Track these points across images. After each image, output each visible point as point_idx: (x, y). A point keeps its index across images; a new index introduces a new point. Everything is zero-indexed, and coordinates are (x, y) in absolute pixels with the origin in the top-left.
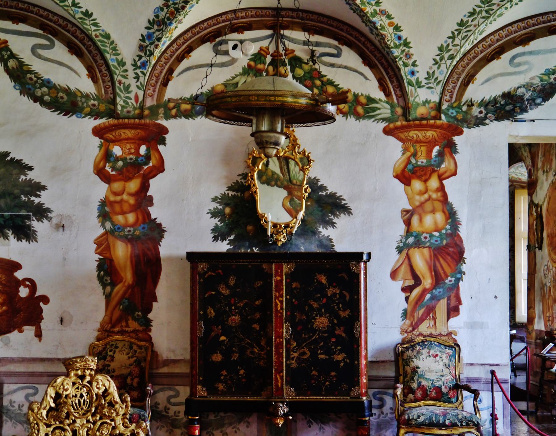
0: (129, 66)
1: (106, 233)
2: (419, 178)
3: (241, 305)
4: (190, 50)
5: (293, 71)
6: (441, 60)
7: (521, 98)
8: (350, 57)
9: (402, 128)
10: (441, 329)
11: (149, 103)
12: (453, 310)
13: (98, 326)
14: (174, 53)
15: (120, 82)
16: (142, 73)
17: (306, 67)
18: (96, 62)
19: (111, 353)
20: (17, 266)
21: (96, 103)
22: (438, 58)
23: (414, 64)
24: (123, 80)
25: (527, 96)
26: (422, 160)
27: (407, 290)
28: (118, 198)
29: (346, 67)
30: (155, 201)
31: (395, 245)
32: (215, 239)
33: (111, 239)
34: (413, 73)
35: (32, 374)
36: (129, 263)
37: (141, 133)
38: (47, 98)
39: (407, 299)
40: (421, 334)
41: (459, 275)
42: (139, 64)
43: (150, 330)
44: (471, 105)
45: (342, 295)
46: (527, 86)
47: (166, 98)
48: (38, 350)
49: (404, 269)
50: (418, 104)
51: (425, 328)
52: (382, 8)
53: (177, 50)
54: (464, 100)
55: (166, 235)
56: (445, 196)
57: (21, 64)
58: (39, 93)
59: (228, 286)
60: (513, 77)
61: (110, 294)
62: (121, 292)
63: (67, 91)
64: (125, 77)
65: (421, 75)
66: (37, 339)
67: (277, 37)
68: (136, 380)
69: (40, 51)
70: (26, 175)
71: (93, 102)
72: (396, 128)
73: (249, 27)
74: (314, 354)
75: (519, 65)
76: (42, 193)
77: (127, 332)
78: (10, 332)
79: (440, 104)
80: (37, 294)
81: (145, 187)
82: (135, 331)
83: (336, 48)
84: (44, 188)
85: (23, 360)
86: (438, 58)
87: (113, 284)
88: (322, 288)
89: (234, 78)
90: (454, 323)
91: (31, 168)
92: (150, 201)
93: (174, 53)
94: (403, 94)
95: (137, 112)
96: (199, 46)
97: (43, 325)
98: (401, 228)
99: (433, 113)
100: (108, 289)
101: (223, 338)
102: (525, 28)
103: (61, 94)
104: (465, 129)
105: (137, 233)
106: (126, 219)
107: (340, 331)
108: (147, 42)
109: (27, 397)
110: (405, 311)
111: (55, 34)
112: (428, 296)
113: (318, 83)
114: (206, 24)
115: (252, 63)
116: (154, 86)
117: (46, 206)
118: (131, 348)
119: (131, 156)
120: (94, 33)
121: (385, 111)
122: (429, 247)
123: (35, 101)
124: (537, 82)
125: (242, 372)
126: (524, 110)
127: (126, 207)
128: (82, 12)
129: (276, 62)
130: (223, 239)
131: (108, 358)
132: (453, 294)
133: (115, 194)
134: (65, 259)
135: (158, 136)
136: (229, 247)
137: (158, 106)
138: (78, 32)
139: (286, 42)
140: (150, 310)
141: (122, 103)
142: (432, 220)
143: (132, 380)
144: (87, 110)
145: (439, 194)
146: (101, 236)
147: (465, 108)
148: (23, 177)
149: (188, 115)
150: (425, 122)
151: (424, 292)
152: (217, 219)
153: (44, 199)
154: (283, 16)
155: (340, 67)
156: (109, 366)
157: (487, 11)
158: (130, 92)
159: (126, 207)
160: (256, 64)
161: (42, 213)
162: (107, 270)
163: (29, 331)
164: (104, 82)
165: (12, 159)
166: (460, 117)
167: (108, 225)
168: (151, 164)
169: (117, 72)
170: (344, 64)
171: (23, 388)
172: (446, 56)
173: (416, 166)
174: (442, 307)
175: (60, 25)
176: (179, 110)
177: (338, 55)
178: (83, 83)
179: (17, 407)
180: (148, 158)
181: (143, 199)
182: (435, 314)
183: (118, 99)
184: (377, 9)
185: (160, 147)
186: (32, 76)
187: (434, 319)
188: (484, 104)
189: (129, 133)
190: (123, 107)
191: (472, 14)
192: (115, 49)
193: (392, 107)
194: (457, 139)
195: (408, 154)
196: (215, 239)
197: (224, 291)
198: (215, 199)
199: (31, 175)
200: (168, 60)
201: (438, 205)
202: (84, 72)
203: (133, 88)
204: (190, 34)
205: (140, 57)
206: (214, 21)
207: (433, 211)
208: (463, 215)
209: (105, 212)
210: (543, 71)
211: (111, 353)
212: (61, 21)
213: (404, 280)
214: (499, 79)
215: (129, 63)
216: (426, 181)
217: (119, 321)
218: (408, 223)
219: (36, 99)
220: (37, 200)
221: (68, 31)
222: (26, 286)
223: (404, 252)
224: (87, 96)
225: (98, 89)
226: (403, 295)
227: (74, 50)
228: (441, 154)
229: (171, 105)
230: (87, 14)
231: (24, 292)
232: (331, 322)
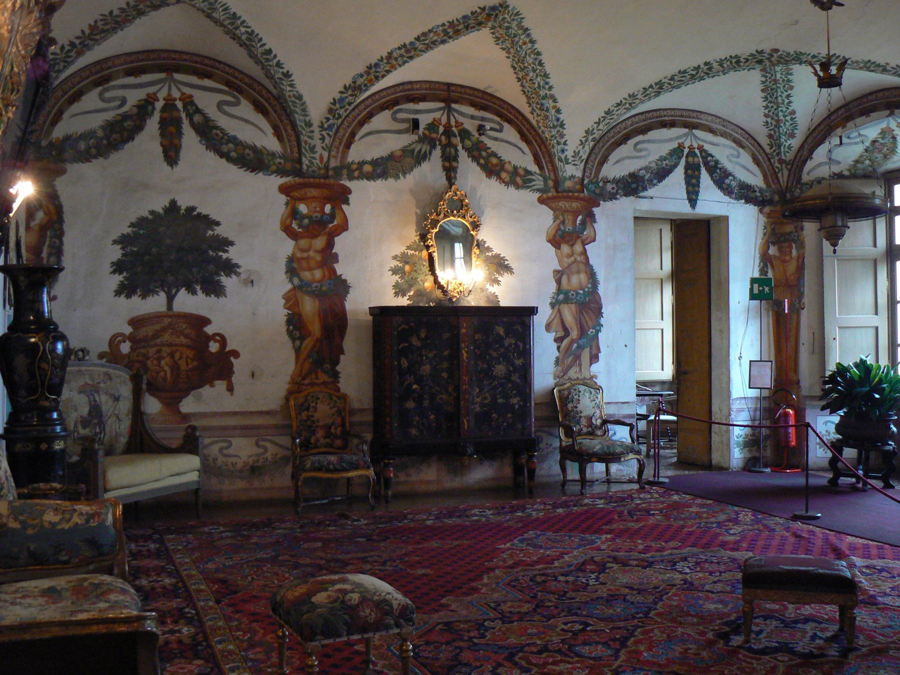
0: (315, 128)
1: (294, 288)
2: (567, 242)
3: (431, 355)
4: (370, 116)
5: (462, 141)
6: (586, 141)
7: (643, 178)
8: (510, 133)
9: (553, 198)
10: (585, 374)
11: (333, 163)
12: (594, 358)
13: (288, 379)
14: (355, 118)
15: (306, 142)
16: (328, 134)
17: (474, 139)
18: (282, 121)
19: (313, 404)
20: (206, 321)
21: (282, 161)
22: (584, 140)
23: (565, 144)
24: (309, 141)
25: (646, 177)
26: (569, 227)
27: (558, 340)
28: (305, 255)
29: (507, 142)
30: (340, 258)
31: (549, 301)
32: (396, 294)
33: (299, 294)
34: (563, 151)
35: (225, 428)
36: (317, 318)
37: (326, 192)
38: (233, 154)
39: (558, 348)
40: (570, 379)
41: (598, 327)
42: (326, 126)
43: (338, 382)
44: (606, 181)
45: (517, 346)
46: (646, 168)
47: (350, 159)
48: (229, 403)
49: (557, 321)
50: (565, 178)
51: (573, 373)
52: (552, 93)
53: (358, 115)
54: (601, 176)
55: (351, 290)
56: (587, 258)
57: (207, 119)
58: (225, 149)
59: (419, 338)
60: (635, 160)
61: (300, 348)
62: (309, 347)
63: (254, 148)
64: (311, 138)
65: (569, 153)
66: (228, 393)
67: (450, 111)
68: (339, 429)
69: (226, 108)
70: (213, 230)
71: (279, 160)
72: (549, 198)
73: (423, 99)
74: (494, 399)
75: (640, 150)
76: (230, 249)
77: (317, 384)
78: (201, 387)
79: (583, 179)
80: (227, 349)
81: (330, 244)
82: (325, 383)
83: (499, 124)
84: (232, 243)
86: (584, 140)
87: (302, 338)
88: (499, 339)
89: (410, 145)
90: (595, 368)
91: (218, 224)
92: (335, 258)
93: (355, 118)
94: (555, 169)
95: (322, 172)
96: (378, 113)
97: (234, 379)
98: (553, 287)
99: (578, 187)
100: (298, 343)
101: (415, 386)
102: (644, 120)
103: (247, 151)
104: (601, 202)
105: (324, 288)
106: (313, 275)
107: (515, 378)
108: (338, 106)
109: (221, 450)
110: (558, 358)
111: (240, 91)
112: (575, 345)
113: (484, 154)
114: (385, 93)
115: (427, 132)
116: (338, 148)
117: (234, 262)
118: (331, 399)
119: (317, 214)
120: (288, 94)
121: (539, 183)
122: (576, 303)
123: (221, 157)
124: (653, 165)
125: (432, 417)
126: (645, 189)
127: (313, 263)
128: (283, 73)
129: (448, 132)
130: (404, 295)
131: (311, 410)
132: (594, 344)
133: (303, 251)
134: (254, 314)
135: (342, 196)
136: (409, 302)
137: (342, 167)
138: (264, 91)
139: (456, 115)
140: (337, 362)
141: (307, 162)
142: (577, 280)
143: (336, 428)
144: (274, 168)
145: (583, 257)
146: (290, 291)
147: (601, 184)
148: (210, 232)
149: (370, 177)
150: (571, 194)
151: (572, 342)
152: (398, 276)
153: (232, 254)
154: (453, 91)
155: (502, 141)
156: (313, 416)
157: (630, 104)
158: (315, 153)
159: (313, 263)
160: (430, 133)
161: (230, 268)
162: (296, 324)
163: (220, 385)
164: (289, 141)
165: (199, 214)
166: (598, 191)
167: (296, 281)
168: (335, 223)
169: (304, 132)
170: (506, 138)
171: (216, 442)
172: (590, 138)
173: (564, 232)
174: (586, 355)
175: (246, 84)
176: (361, 172)
177: (500, 131)
178: (271, 143)
179: (211, 460)
180: (332, 216)
181: (329, 257)
182: (580, 361)
183: (304, 159)
184: (548, 93)
185: (344, 207)
186: (218, 132)
187: (580, 365)
188: (616, 181)
189: (314, 192)
190: (308, 167)
191: (618, 105)
192: (304, 110)
193: (545, 180)
194: (596, 210)
195: (558, 221)
196: (396, 294)
197: (415, 342)
198: (395, 258)
199: (218, 230)
200: (350, 124)
201: (582, 267)
202: (269, 130)
203: (318, 149)
204: (370, 101)
205: (328, 119)
206: (393, 90)
207: (578, 272)
208: (600, 277)
209: (292, 269)
210: (657, 158)
211: (313, 404)
212: (246, 80)
213: (556, 332)
214: (627, 161)
215: (316, 124)
216: (572, 246)
217: (309, 373)
218: (559, 282)
219: (222, 155)
220: (225, 256)
221: (254, 90)
223: (557, 307)
224: (273, 154)
225: (284, 147)
226: (555, 345)
227: (260, 108)
228: (583, 223)
229: (354, 167)
230: (287, 75)
231: (214, 347)
232: (508, 369)
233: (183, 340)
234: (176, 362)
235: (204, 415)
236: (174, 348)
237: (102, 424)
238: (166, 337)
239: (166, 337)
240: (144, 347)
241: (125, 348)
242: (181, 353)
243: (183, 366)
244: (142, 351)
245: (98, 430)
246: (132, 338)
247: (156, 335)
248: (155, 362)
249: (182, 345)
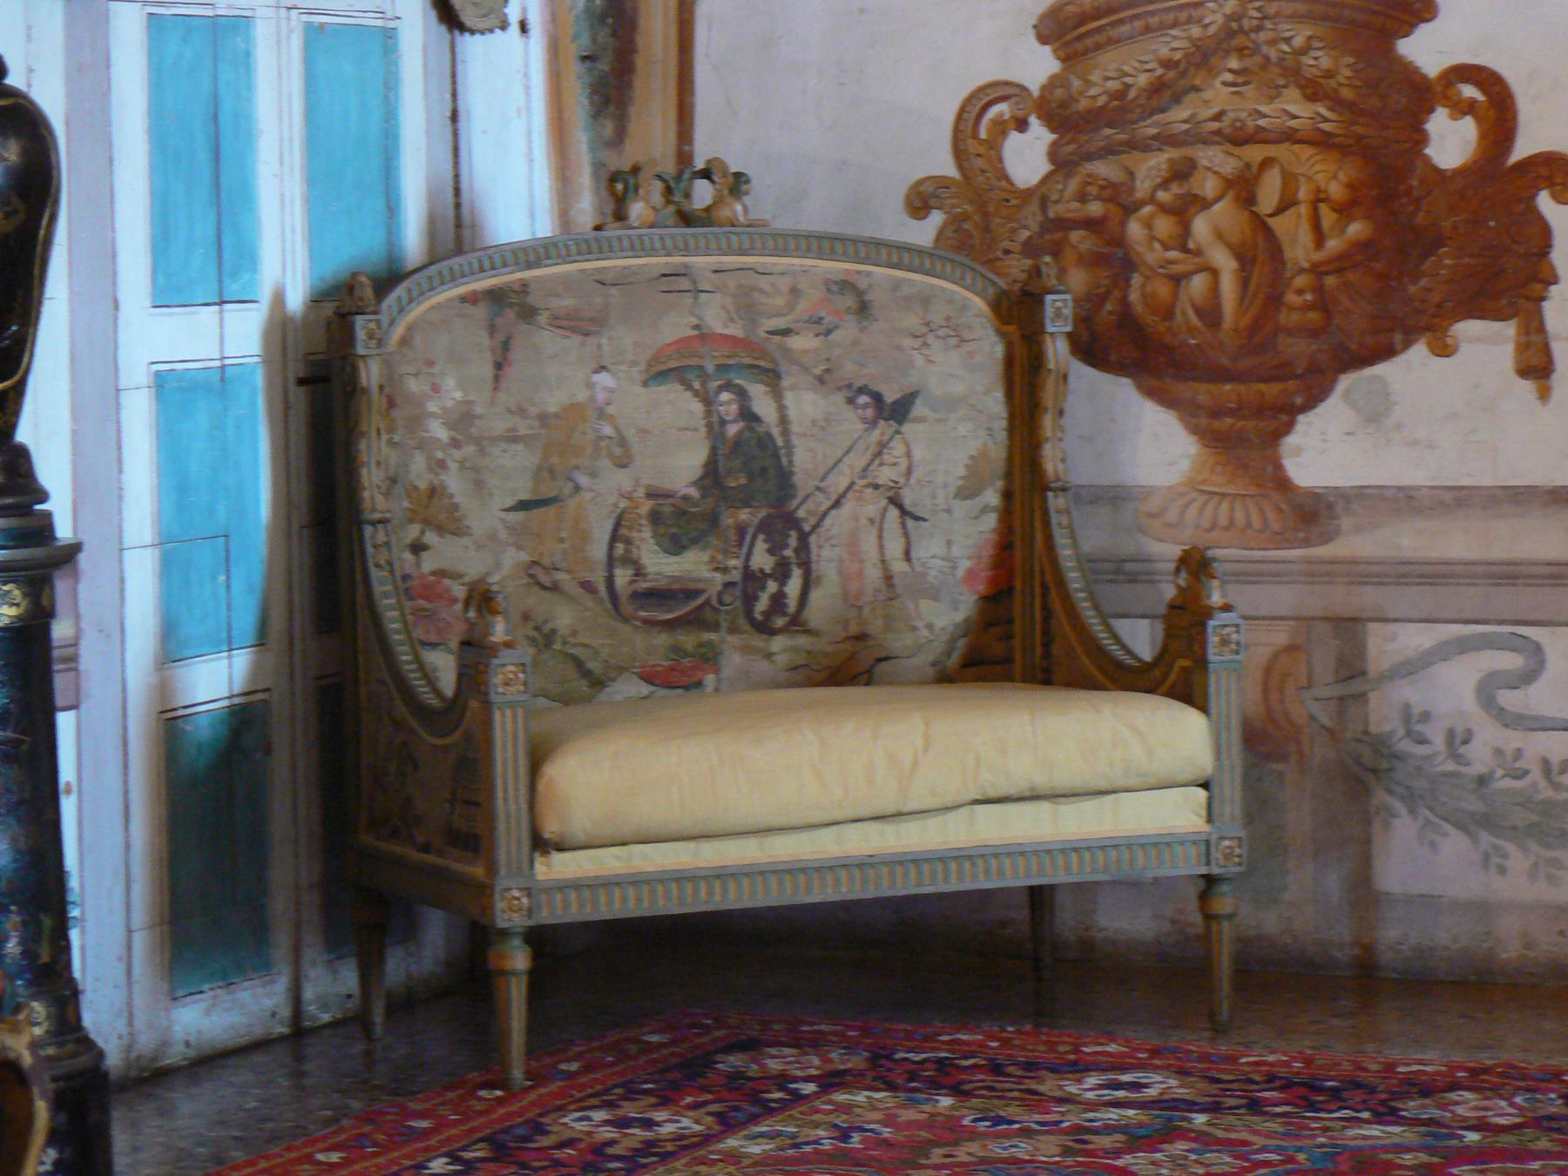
35: (1508, 574)
66: (1527, 387)
78: (1387, 352)
80: (1521, 150)
85: (1459, 500)
109: (1487, 690)
163: (1486, 344)
171: (1463, 646)
179: (1439, 742)
222: (1464, 109)
231: (1451, 141)
233: (1297, 109)
234: (1261, 224)
235: (1404, 502)
236: (1255, 153)
237: (783, 524)
238: (1217, 97)
239: (1217, 97)
240: (1110, 151)
241: (1028, 156)
242: (1289, 179)
243: (1299, 248)
244: (1104, 169)
245: (762, 560)
246: (1056, 109)
247: (1165, 91)
248: (1165, 226)
249: (1290, 136)
